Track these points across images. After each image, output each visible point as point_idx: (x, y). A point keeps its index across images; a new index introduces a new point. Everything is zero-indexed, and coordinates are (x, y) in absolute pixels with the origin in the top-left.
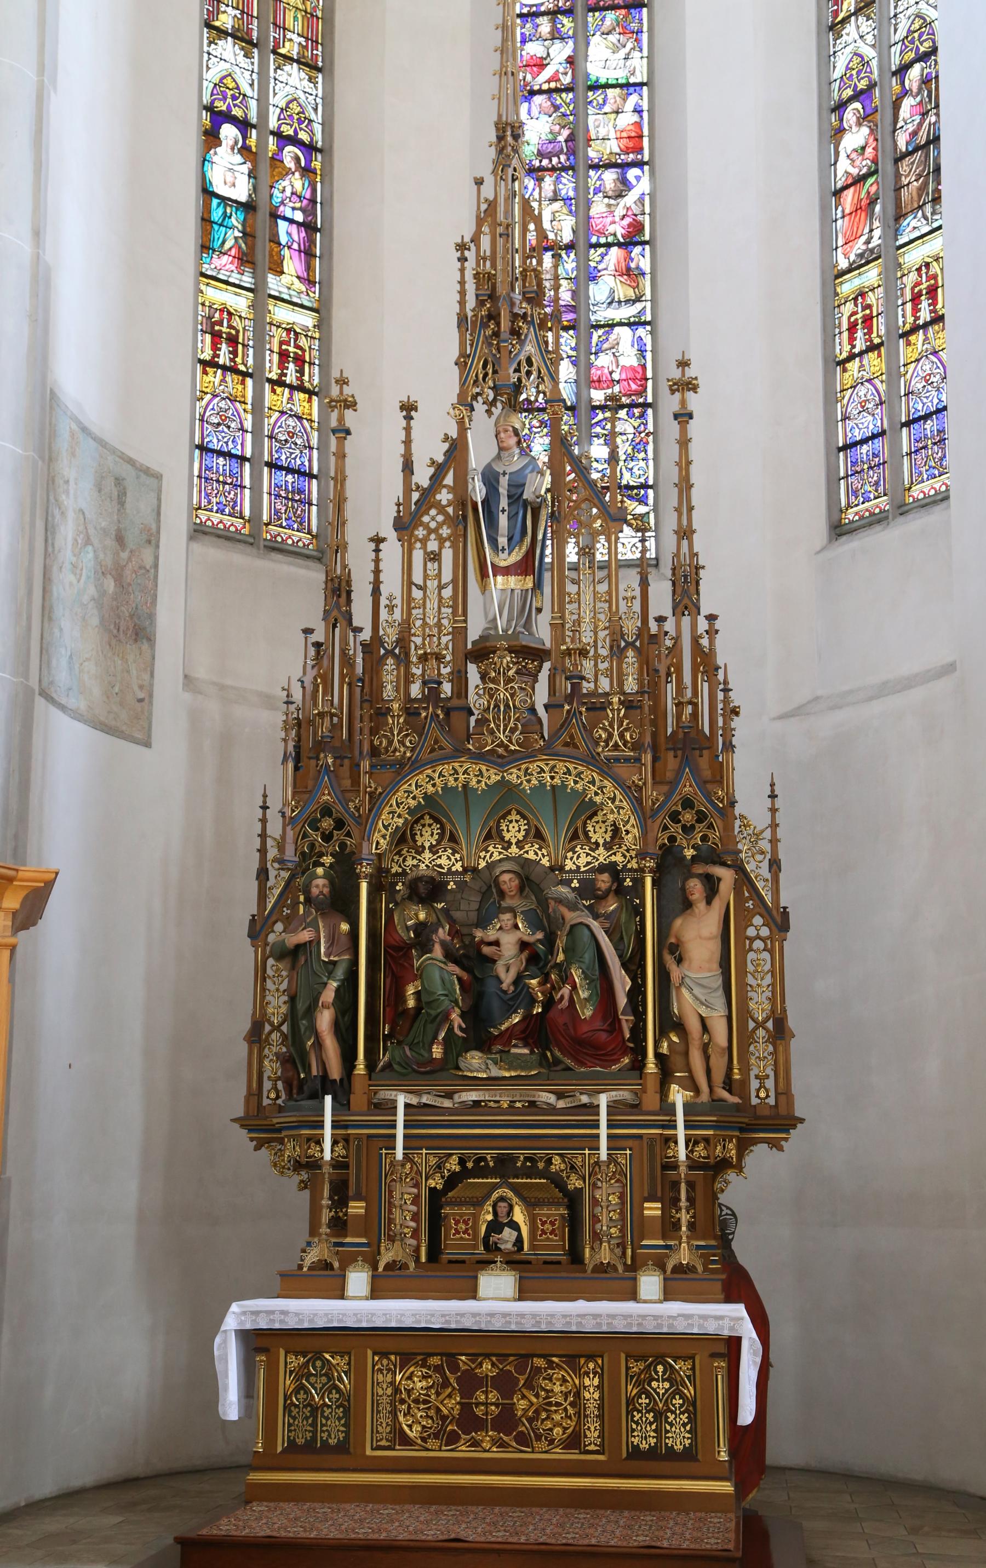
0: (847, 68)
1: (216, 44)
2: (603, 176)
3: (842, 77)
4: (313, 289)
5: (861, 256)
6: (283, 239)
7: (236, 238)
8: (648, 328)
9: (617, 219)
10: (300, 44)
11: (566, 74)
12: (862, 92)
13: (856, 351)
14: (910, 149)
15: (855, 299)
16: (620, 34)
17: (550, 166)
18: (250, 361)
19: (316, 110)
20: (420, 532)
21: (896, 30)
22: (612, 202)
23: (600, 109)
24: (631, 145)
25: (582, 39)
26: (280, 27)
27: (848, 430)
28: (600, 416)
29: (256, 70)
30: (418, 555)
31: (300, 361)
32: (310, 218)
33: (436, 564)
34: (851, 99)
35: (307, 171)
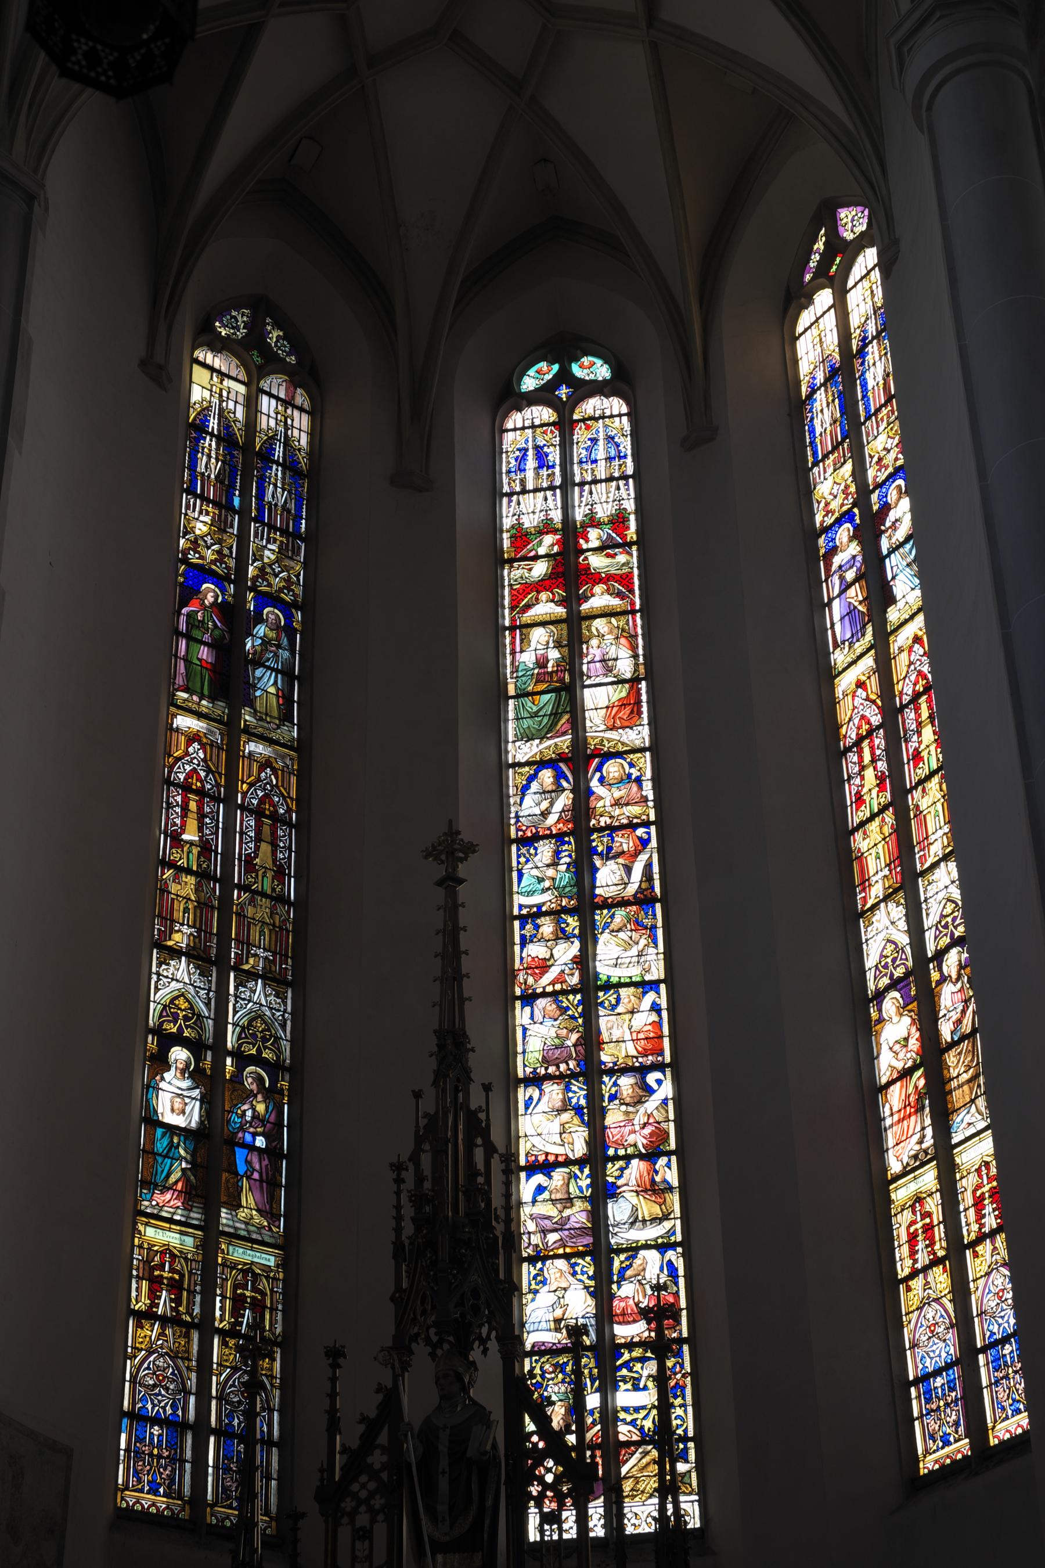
0: (882, 956)
1: (168, 964)
2: (619, 1082)
3: (876, 966)
4: (277, 1223)
5: (915, 1157)
6: (241, 1169)
7: (183, 1170)
8: (680, 1250)
9: (637, 1128)
10: (266, 958)
11: (572, 975)
12: (900, 980)
13: (919, 1266)
14: (956, 1039)
15: (913, 1206)
16: (631, 930)
17: (557, 1073)
18: (197, 1310)
19: (283, 1026)
20: (348, 1504)
21: (928, 915)
22: (630, 1109)
23: (613, 1010)
24: (649, 1046)
25: (588, 937)
26: (243, 944)
27: (918, 1360)
28: (626, 1356)
29: (213, 989)
30: (345, 1533)
31: (258, 1307)
32: (274, 1144)
33: (367, 1543)
34: (888, 988)
35: (271, 1094)
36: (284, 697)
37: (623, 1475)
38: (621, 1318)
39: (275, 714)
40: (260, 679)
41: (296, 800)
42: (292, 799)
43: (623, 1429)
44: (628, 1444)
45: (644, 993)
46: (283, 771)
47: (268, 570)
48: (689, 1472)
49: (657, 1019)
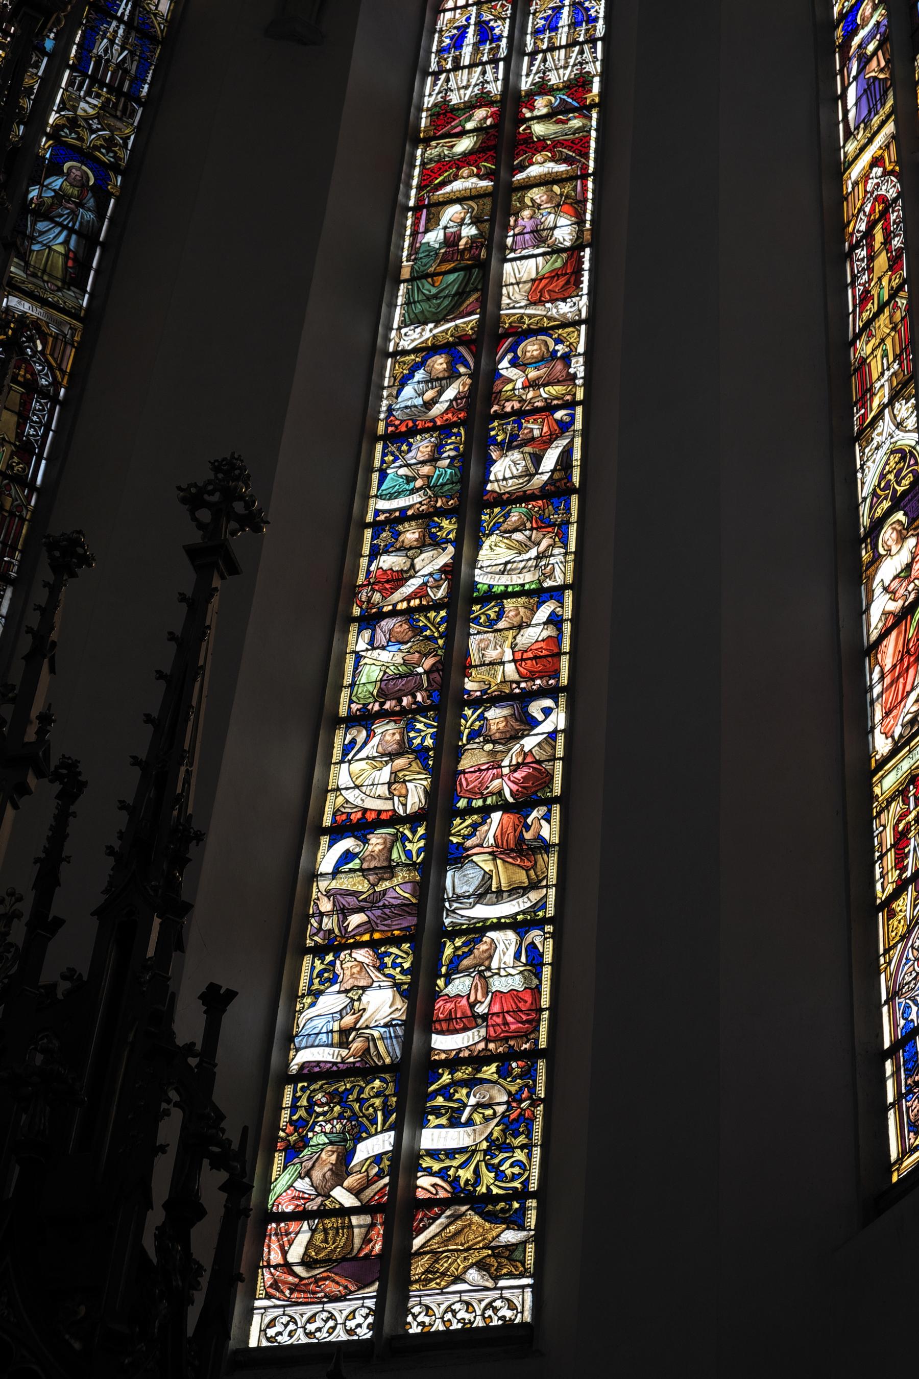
2: (486, 714)
8: (549, 928)
9: (506, 771)
11: (438, 587)
16: (532, 529)
17: (398, 709)
22: (500, 748)
23: (491, 626)
24: (539, 667)
28: (446, 1078)
36: (75, 260)
37: (415, 1248)
38: (444, 1026)
39: (59, 274)
40: (42, 233)
41: (70, 375)
42: (63, 372)
43: (424, 1181)
44: (430, 1203)
45: (540, 604)
46: (56, 338)
47: (83, 123)
48: (524, 1243)
49: (554, 634)
